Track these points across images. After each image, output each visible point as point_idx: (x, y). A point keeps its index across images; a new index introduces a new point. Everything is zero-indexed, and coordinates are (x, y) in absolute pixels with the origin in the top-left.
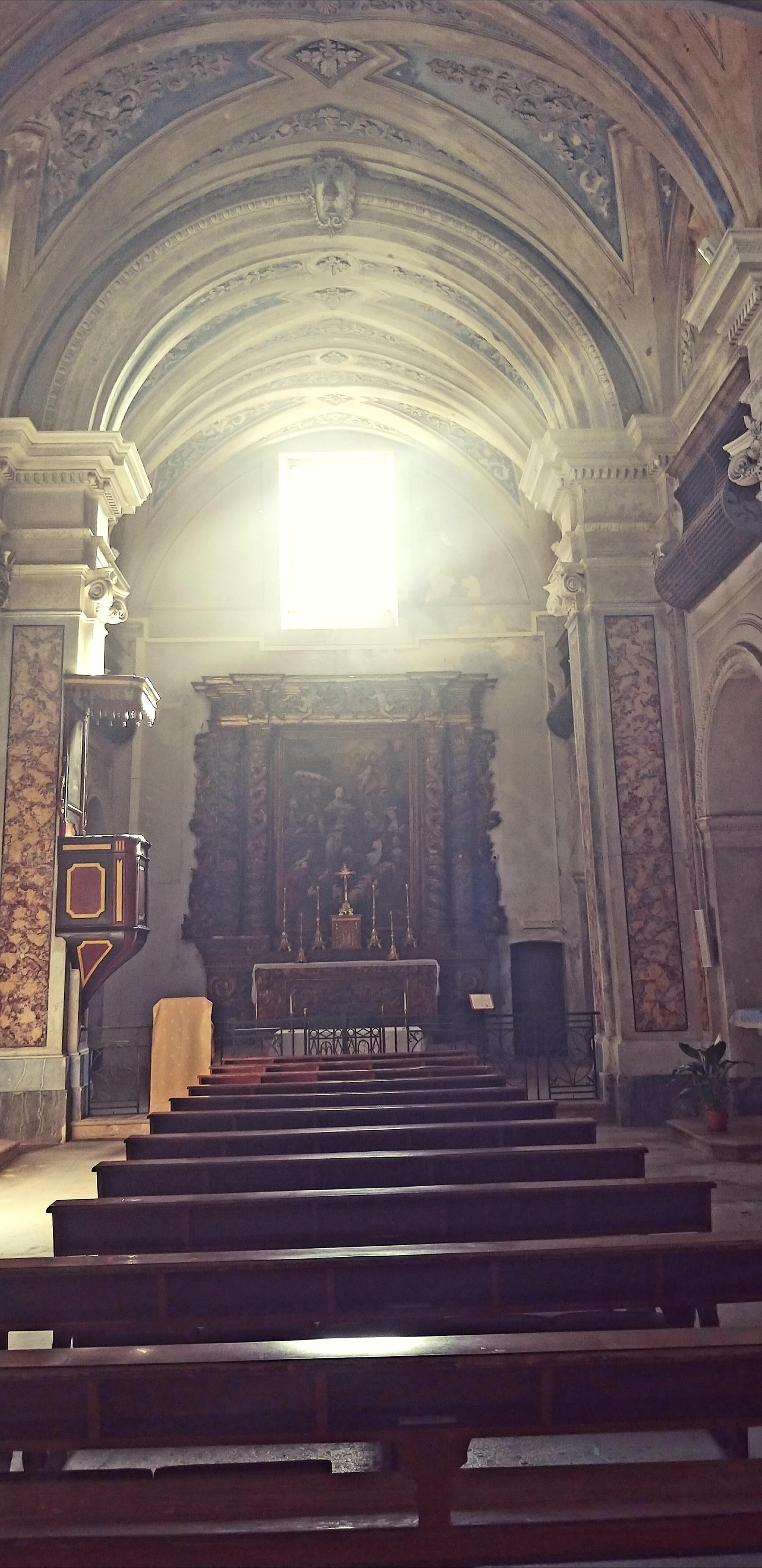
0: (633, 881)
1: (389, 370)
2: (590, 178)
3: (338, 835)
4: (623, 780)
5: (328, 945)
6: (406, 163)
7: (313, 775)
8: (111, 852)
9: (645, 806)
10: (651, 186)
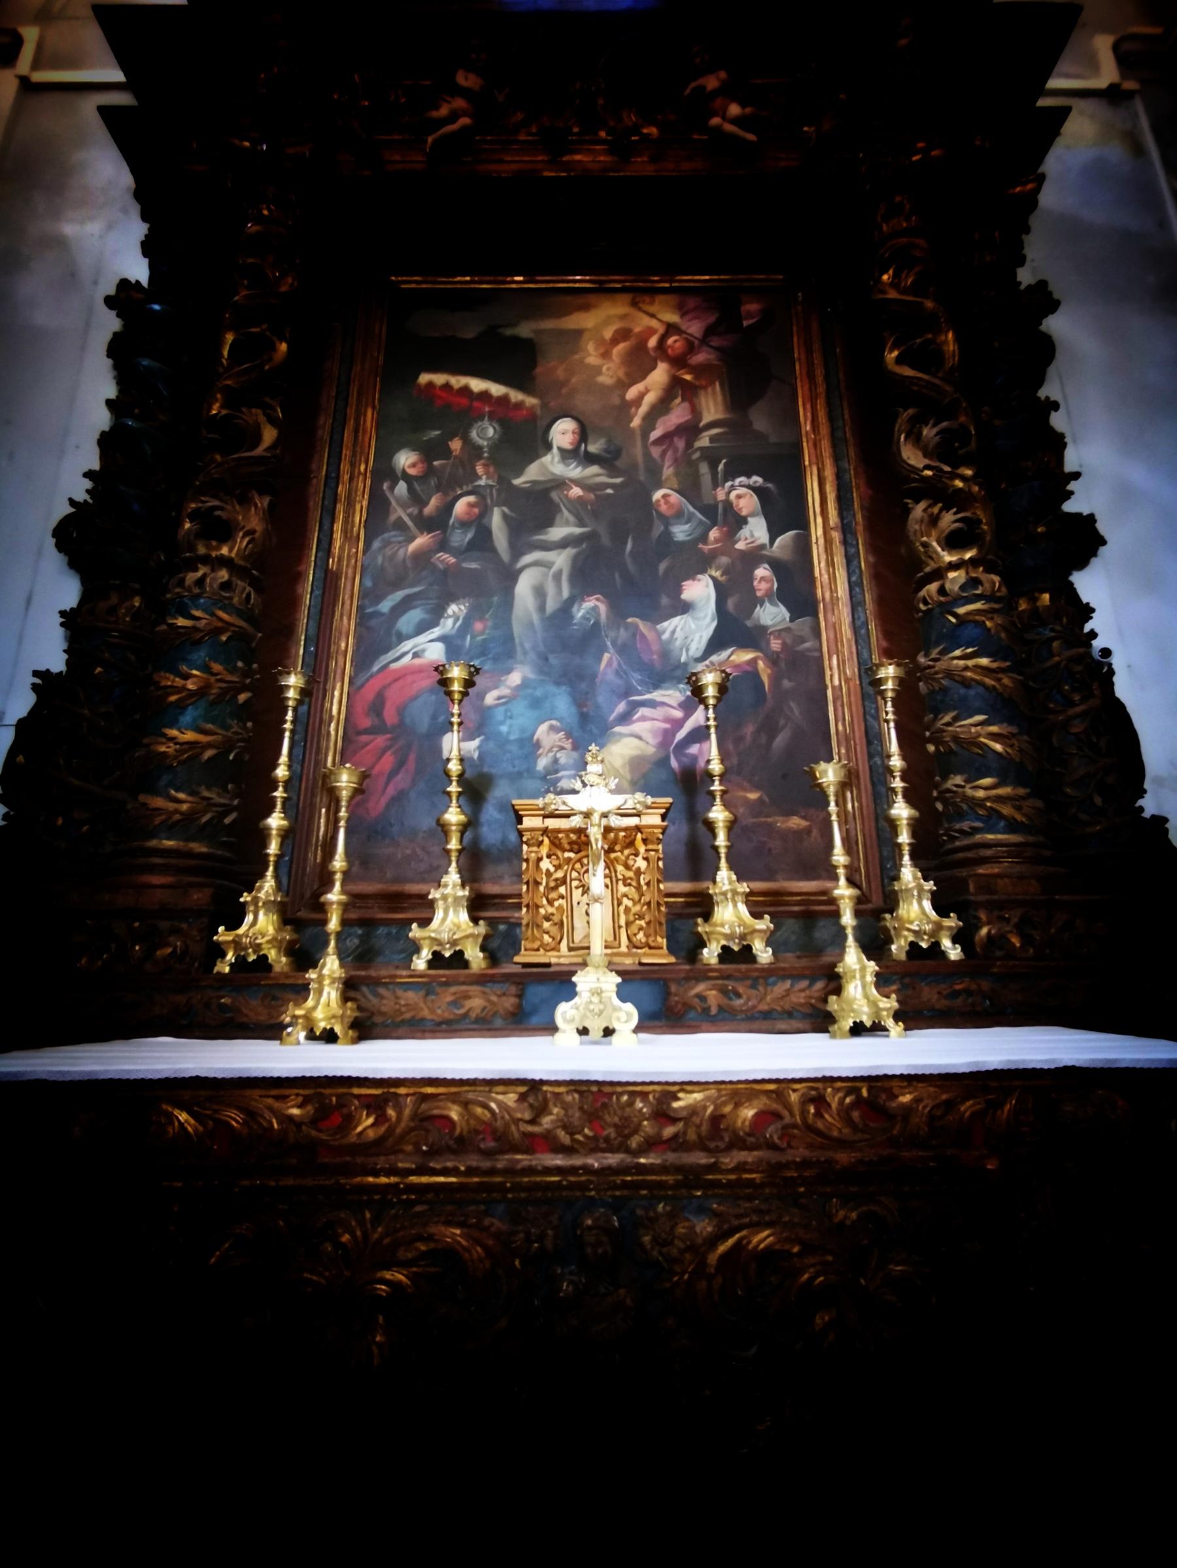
3: (561, 560)
5: (499, 945)
7: (477, 385)
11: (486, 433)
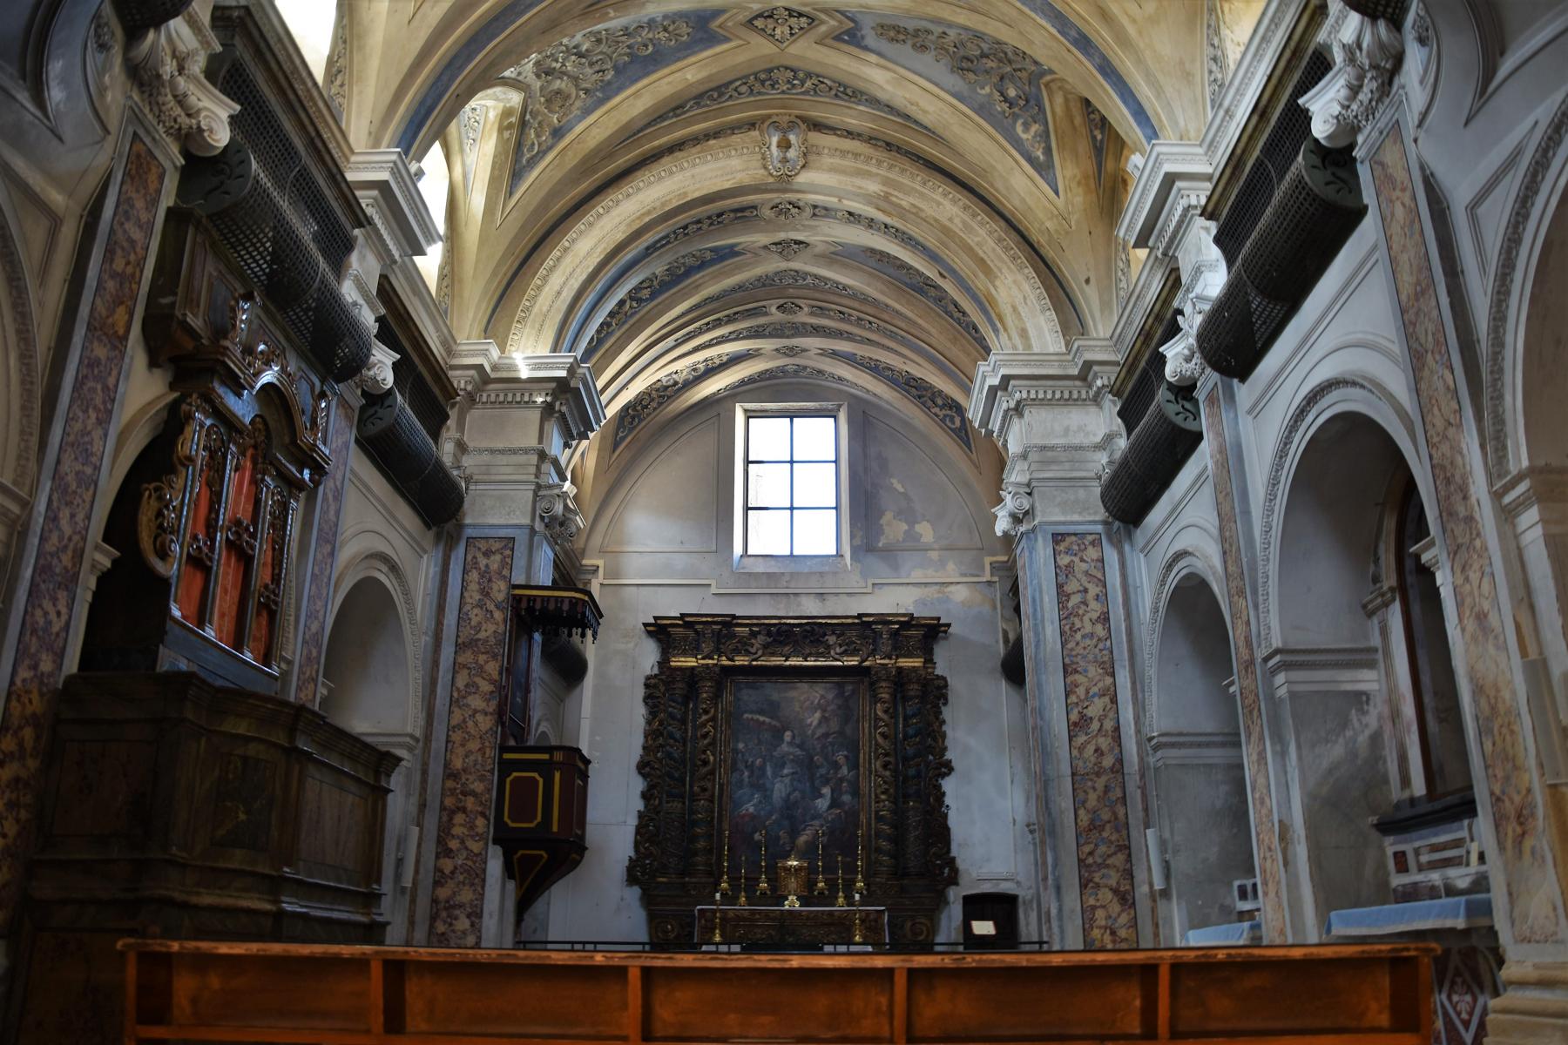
0: (1084, 802)
1: (842, 320)
2: (1026, 126)
3: (787, 780)
4: (1073, 699)
5: (774, 888)
6: (855, 116)
8: (550, 762)
9: (1095, 726)
11: (767, 736)
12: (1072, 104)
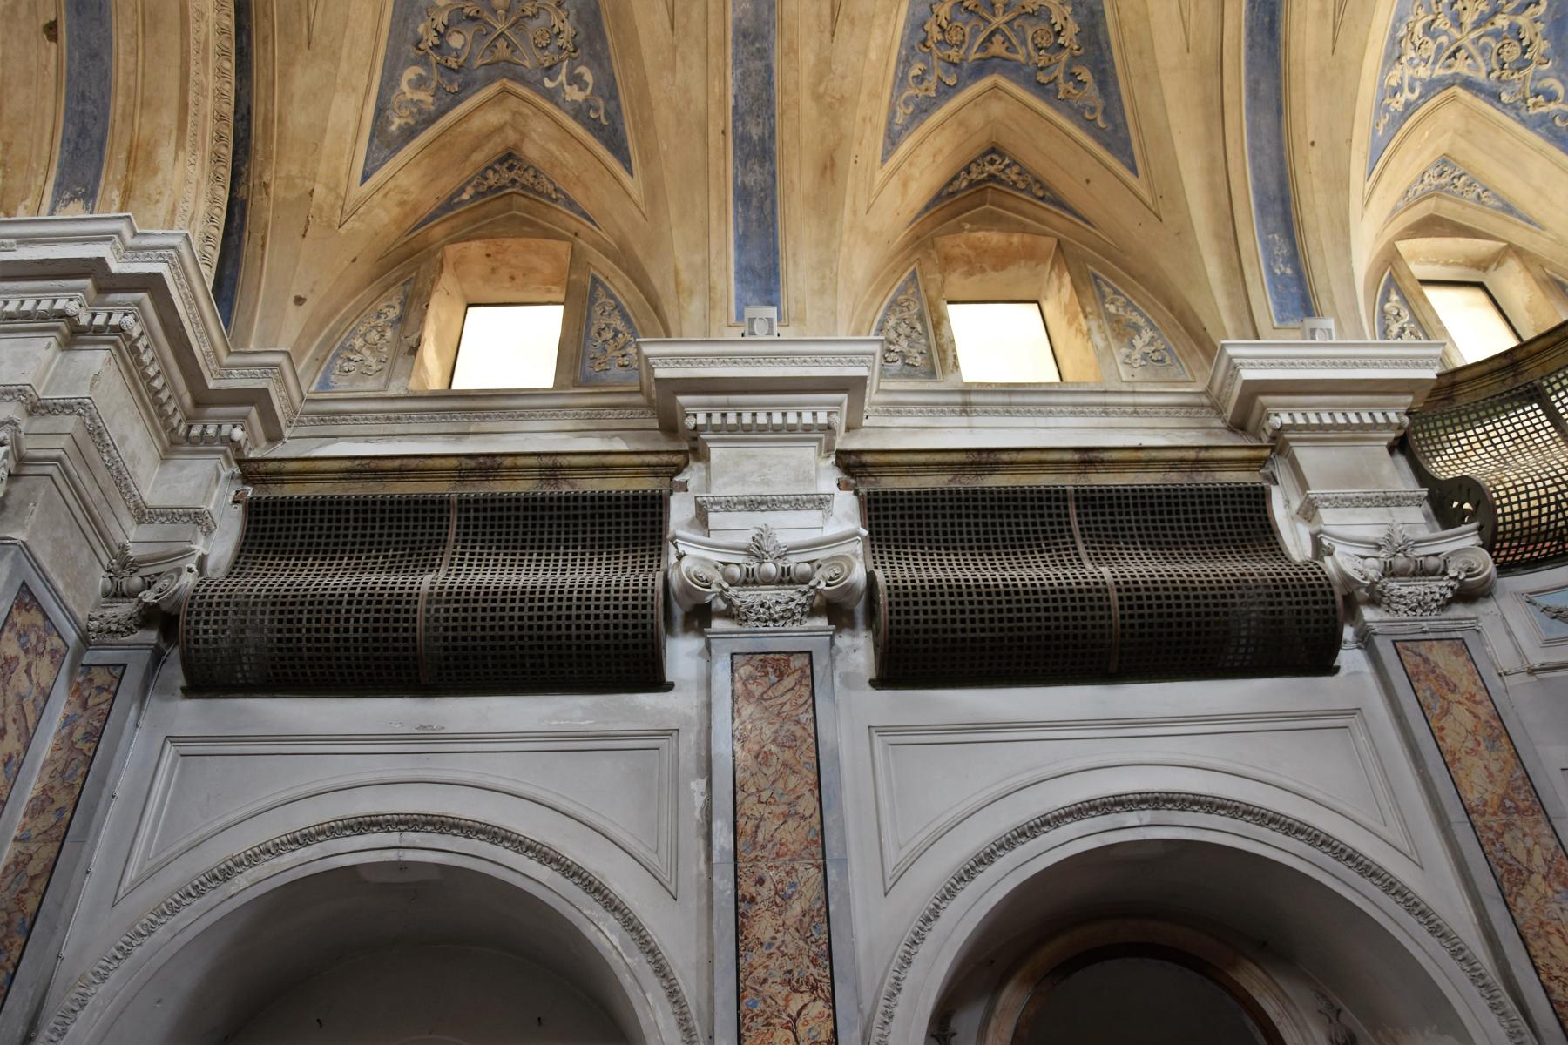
2: (419, 83)
10: (468, 172)
12: (497, 139)
